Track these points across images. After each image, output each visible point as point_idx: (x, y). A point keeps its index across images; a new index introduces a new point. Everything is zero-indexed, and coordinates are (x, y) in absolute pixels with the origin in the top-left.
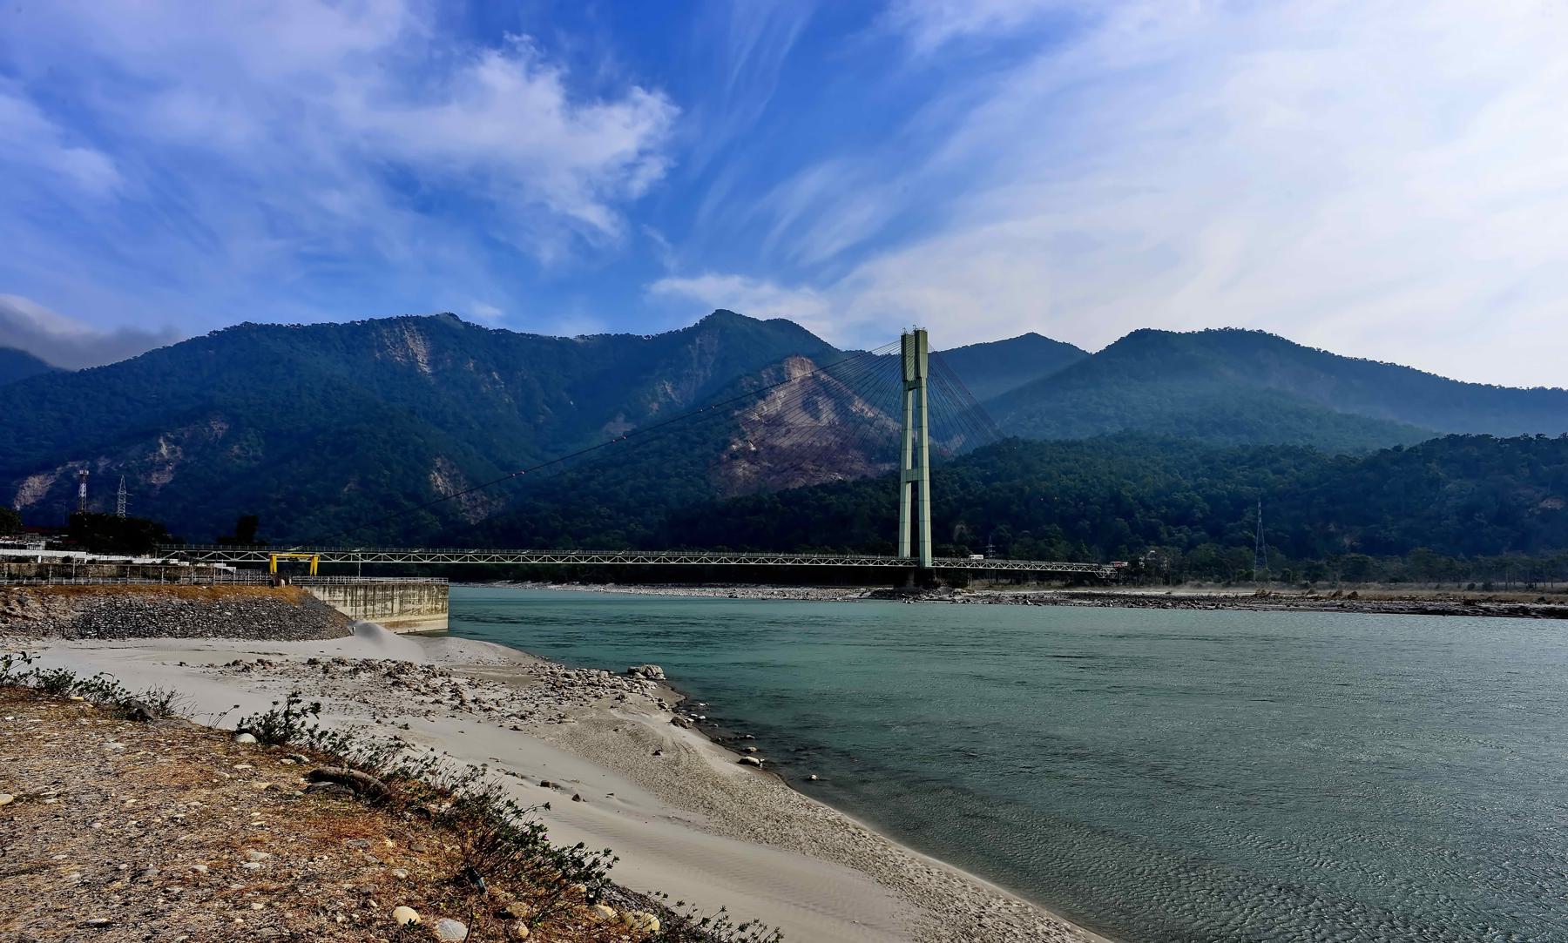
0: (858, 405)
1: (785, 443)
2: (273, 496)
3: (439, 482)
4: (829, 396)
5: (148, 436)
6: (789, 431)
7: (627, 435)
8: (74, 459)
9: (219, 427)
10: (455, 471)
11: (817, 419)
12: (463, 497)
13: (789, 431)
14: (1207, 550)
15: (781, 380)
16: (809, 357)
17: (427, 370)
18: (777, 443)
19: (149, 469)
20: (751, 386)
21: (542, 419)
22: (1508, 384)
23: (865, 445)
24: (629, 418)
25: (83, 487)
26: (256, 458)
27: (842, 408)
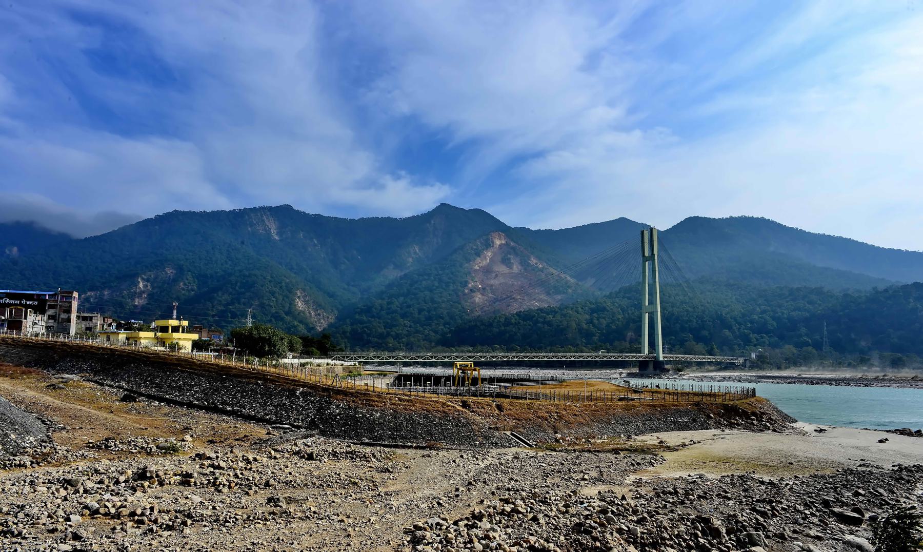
0: (533, 261)
1: (495, 282)
3: (300, 305)
4: (516, 254)
5: (132, 278)
6: (497, 275)
7: (401, 278)
8: (90, 290)
9: (170, 271)
10: (308, 298)
11: (511, 268)
12: (313, 313)
14: (789, 349)
17: (277, 238)
18: (492, 282)
19: (133, 296)
20: (472, 249)
22: (910, 249)
23: (542, 284)
25: (175, 312)
26: (193, 290)
27: (524, 263)
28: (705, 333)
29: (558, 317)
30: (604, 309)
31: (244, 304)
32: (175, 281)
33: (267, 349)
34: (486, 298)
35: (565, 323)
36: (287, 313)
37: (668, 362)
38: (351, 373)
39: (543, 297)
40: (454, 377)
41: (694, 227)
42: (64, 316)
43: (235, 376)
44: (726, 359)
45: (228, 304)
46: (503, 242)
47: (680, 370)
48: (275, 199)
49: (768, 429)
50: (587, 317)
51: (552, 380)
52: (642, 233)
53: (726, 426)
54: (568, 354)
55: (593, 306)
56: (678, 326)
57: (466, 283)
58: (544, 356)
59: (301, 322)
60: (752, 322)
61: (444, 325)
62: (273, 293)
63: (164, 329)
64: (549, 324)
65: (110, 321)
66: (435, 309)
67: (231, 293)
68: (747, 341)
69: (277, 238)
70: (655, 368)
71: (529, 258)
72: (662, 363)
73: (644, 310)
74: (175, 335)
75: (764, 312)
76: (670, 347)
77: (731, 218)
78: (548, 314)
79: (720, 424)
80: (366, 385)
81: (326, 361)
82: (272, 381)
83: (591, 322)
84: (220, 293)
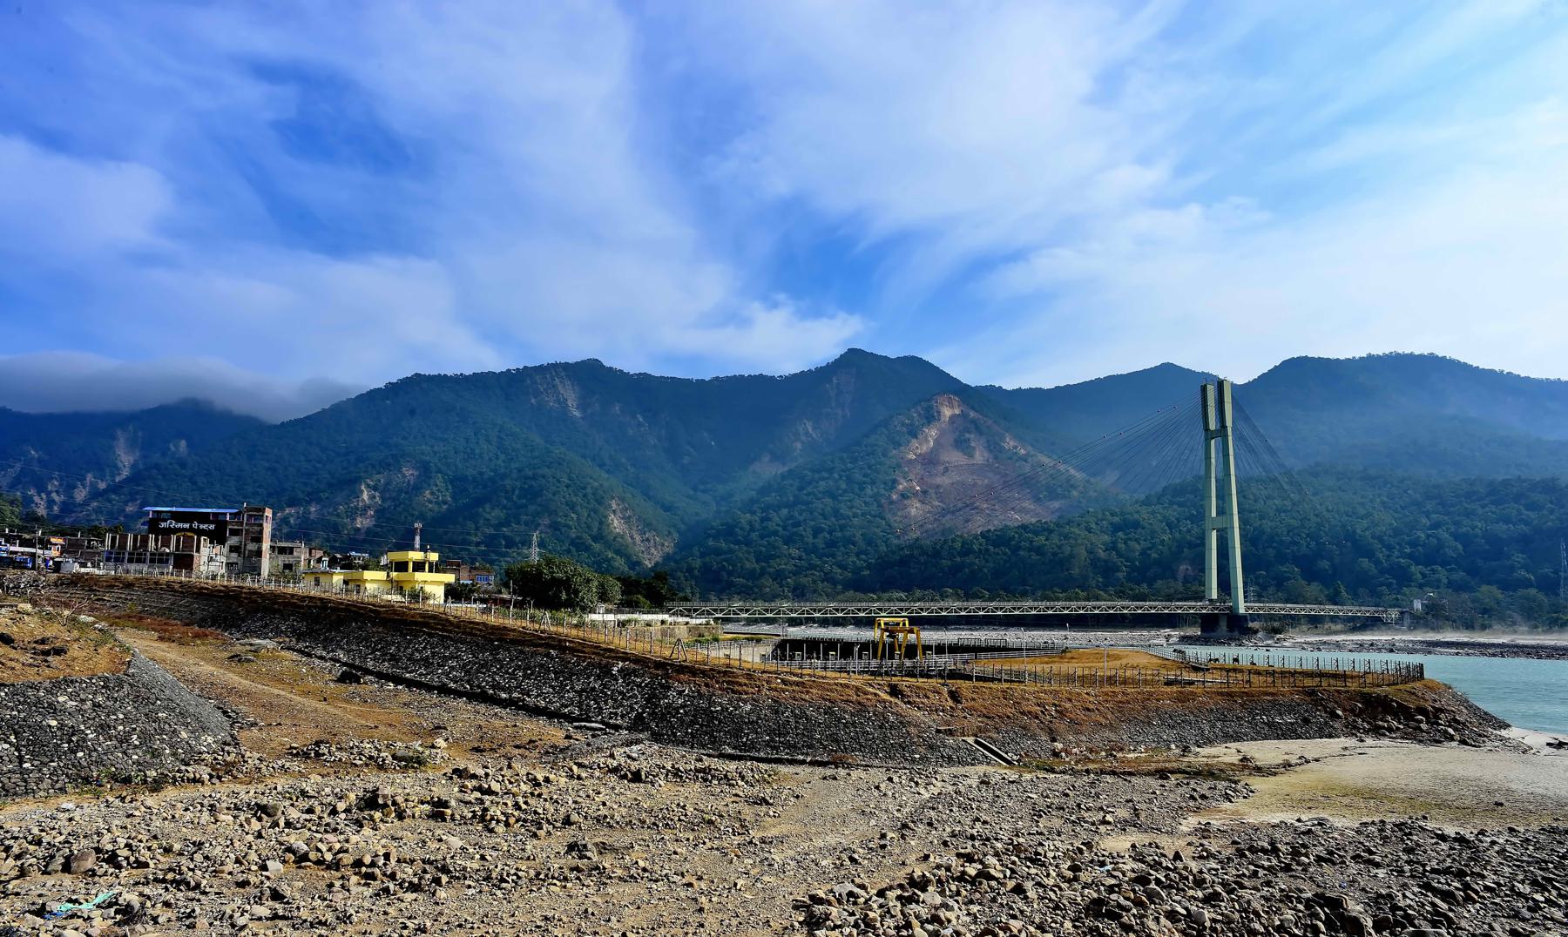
0: (1009, 443)
1: (943, 481)
2: (474, 539)
3: (616, 524)
4: (981, 433)
5: (349, 484)
6: (946, 469)
7: (783, 477)
9: (409, 473)
10: (629, 513)
11: (971, 456)
12: (638, 538)
13: (946, 469)
14: (1489, 593)
15: (931, 417)
16: (955, 394)
17: (577, 414)
19: (353, 513)
21: (686, 460)
24: (777, 457)
25: (418, 538)
27: (994, 448)
28: (1324, 564)
29: (1055, 539)
30: (1136, 525)
31: (526, 524)
32: (417, 488)
33: (564, 596)
34: (928, 508)
35: (1067, 550)
36: (595, 539)
37: (1254, 618)
38: (699, 638)
39: (1028, 505)
40: (875, 644)
41: (1301, 378)
42: (252, 546)
43: (514, 642)
44: (1367, 611)
45: (501, 525)
46: (957, 412)
47: (1276, 631)
48: (574, 351)
49: (1452, 738)
50: (1107, 538)
51: (1046, 650)
52: (1204, 389)
53: (1367, 732)
54: (1074, 604)
55: (1116, 519)
56: (1271, 552)
57: (895, 481)
58: (1030, 607)
59: (617, 552)
60: (1413, 544)
61: (858, 555)
62: (572, 507)
63: (401, 567)
64: (1039, 550)
65: (319, 554)
66: (842, 528)
67: (505, 507)
68: (1403, 578)
69: (577, 414)
70: (1231, 628)
71: (1003, 439)
72: (1244, 617)
73: (1208, 525)
74: (419, 576)
75: (1436, 526)
76: (1259, 585)
77: (1370, 357)
78: (1036, 533)
79: (1355, 727)
80: (728, 656)
81: (661, 617)
82: (572, 650)
83: (1112, 547)
84: (488, 507)
